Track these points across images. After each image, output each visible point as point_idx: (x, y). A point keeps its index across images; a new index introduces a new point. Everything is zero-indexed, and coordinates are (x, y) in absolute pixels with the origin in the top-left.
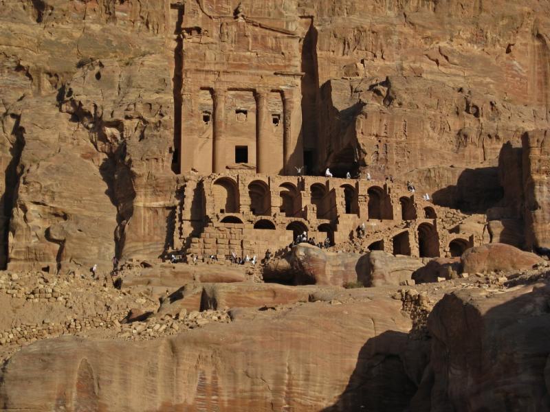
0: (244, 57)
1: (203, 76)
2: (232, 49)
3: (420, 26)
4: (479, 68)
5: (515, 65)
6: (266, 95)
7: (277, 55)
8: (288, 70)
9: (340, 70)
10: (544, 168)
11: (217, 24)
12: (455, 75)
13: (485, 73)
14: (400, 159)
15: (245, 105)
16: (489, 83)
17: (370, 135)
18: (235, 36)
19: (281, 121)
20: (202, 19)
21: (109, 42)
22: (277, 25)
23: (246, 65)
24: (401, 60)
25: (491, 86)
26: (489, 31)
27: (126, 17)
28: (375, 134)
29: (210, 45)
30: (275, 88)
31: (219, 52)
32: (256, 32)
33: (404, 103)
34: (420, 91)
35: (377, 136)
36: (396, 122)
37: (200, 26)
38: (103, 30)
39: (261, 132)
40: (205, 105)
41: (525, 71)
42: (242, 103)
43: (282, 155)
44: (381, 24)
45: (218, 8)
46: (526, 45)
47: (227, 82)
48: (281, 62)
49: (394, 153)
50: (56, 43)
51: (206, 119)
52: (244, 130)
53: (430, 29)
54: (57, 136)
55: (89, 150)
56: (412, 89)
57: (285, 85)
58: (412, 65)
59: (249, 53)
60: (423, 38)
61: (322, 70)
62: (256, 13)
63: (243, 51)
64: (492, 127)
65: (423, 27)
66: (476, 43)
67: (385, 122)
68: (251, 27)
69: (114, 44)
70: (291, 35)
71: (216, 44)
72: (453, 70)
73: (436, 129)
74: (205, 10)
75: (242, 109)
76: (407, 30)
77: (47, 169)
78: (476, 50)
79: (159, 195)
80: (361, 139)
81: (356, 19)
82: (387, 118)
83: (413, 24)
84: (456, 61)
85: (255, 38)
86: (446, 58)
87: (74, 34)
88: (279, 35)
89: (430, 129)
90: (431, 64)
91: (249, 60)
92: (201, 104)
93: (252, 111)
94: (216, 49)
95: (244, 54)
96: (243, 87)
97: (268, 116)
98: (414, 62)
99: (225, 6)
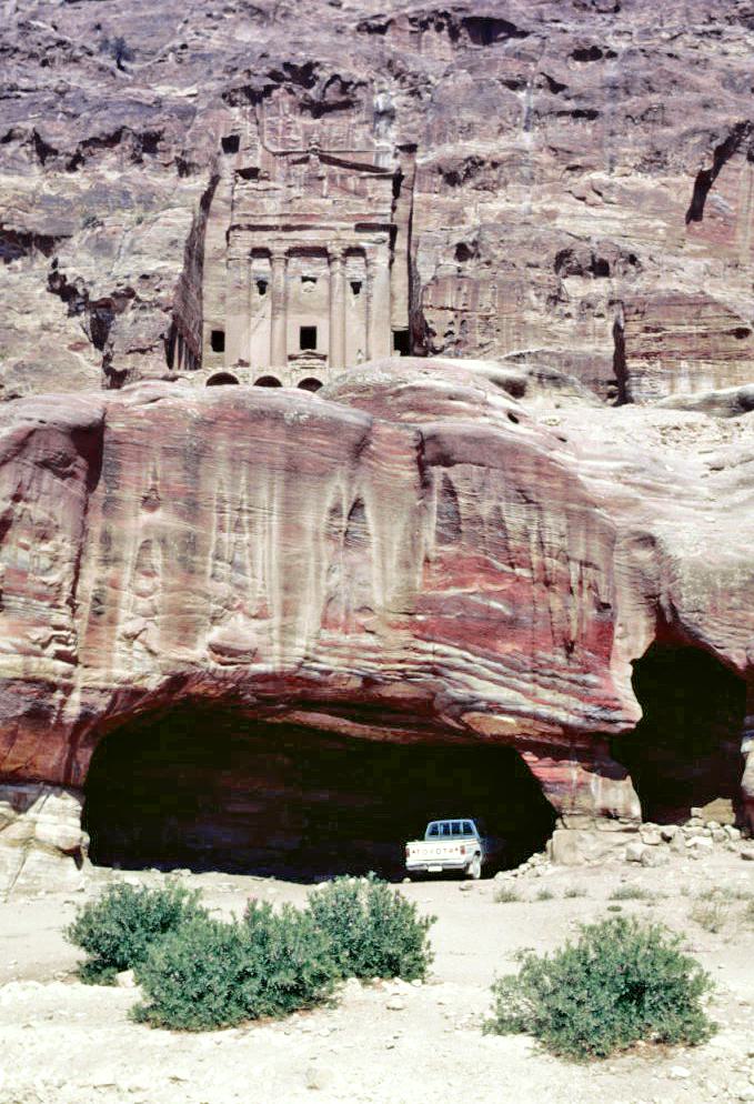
0: (317, 205)
1: (257, 233)
3: (562, 150)
4: (648, 207)
5: (717, 200)
7: (361, 201)
8: (373, 221)
10: (643, 351)
12: (607, 218)
13: (656, 213)
14: (485, 340)
15: (315, 270)
16: (657, 228)
17: (442, 308)
19: (362, 290)
21: (126, 195)
22: (362, 159)
23: (318, 217)
24: (532, 200)
25: (661, 231)
26: (669, 154)
30: (353, 244)
34: (523, 243)
35: (452, 309)
36: (481, 289)
37: (257, 163)
38: (121, 179)
39: (334, 307)
41: (732, 208)
43: (364, 337)
44: (505, 150)
46: (738, 170)
48: (365, 210)
50: (57, 200)
51: (262, 292)
53: (581, 154)
54: (38, 323)
55: (79, 340)
57: (369, 241)
58: (545, 207)
60: (568, 169)
62: (335, 145)
64: (628, 292)
65: (569, 152)
66: (649, 170)
67: (465, 289)
68: (325, 166)
69: (133, 197)
70: (380, 173)
72: (606, 212)
73: (543, 298)
74: (267, 144)
76: (546, 158)
77: (16, 367)
78: (649, 182)
80: (428, 316)
81: (474, 147)
82: (469, 284)
83: (554, 149)
84: (613, 199)
85: (332, 179)
86: (600, 194)
88: (365, 174)
89: (534, 299)
90: (575, 204)
92: (255, 272)
96: (309, 244)
98: (549, 202)
99: (294, 137)
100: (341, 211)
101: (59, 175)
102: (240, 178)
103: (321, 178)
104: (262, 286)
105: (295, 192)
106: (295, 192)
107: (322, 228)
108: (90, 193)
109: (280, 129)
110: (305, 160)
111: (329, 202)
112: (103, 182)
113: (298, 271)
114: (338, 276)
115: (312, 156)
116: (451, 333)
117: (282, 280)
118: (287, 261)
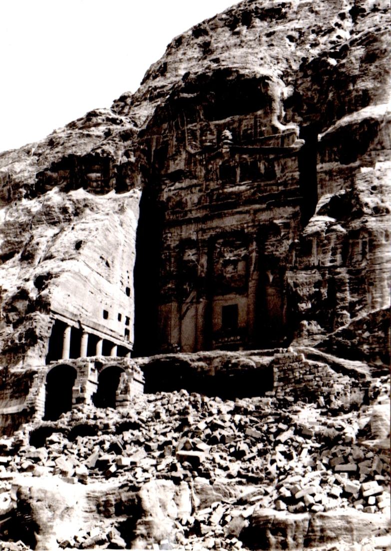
0: (232, 193)
9: (345, 183)
11: (201, 161)
15: (235, 252)
20: (185, 159)
21: (64, 210)
27: (99, 177)
28: (316, 264)
32: (245, 159)
33: (365, 210)
42: (231, 251)
45: (202, 142)
49: (347, 288)
56: (381, 186)
59: (237, 187)
61: (322, 188)
74: (189, 149)
75: (232, 258)
79: (17, 398)
87: (32, 210)
91: (239, 194)
95: (231, 190)
100: (254, 194)
101: (18, 203)
106: (213, 185)
108: (40, 213)
109: (198, 133)
112: (49, 203)
116: (318, 295)
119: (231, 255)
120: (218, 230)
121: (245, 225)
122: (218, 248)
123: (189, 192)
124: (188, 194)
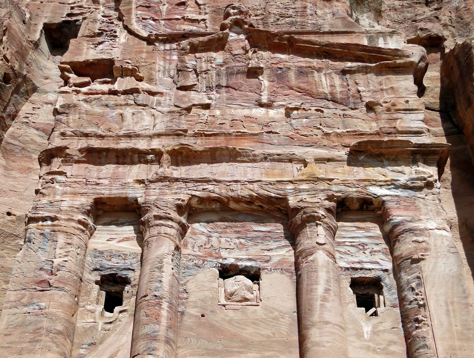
2: (208, 101)
6: (321, 212)
15: (254, 251)
18: (218, 75)
19: (389, 296)
29: (142, 98)
30: (353, 192)
31: (166, 109)
40: (111, 255)
42: (241, 247)
47: (185, 181)
52: (248, 332)
63: (243, 107)
71: (161, 94)
74: (136, 26)
85: (280, 75)
93: (280, 267)
94: (159, 103)
97: (338, 281)
102: (73, 78)
103: (253, 73)
104: (114, 288)
105: (196, 97)
106: (196, 97)
107: (265, 158)
110: (218, 44)
111: (276, 114)
113: (214, 253)
114: (321, 257)
115: (233, 36)
117: (168, 269)
118: (183, 229)
119: (242, 254)
120: (210, 187)
121: (290, 186)
122: (203, 233)
123: (132, 102)
124: (127, 105)
